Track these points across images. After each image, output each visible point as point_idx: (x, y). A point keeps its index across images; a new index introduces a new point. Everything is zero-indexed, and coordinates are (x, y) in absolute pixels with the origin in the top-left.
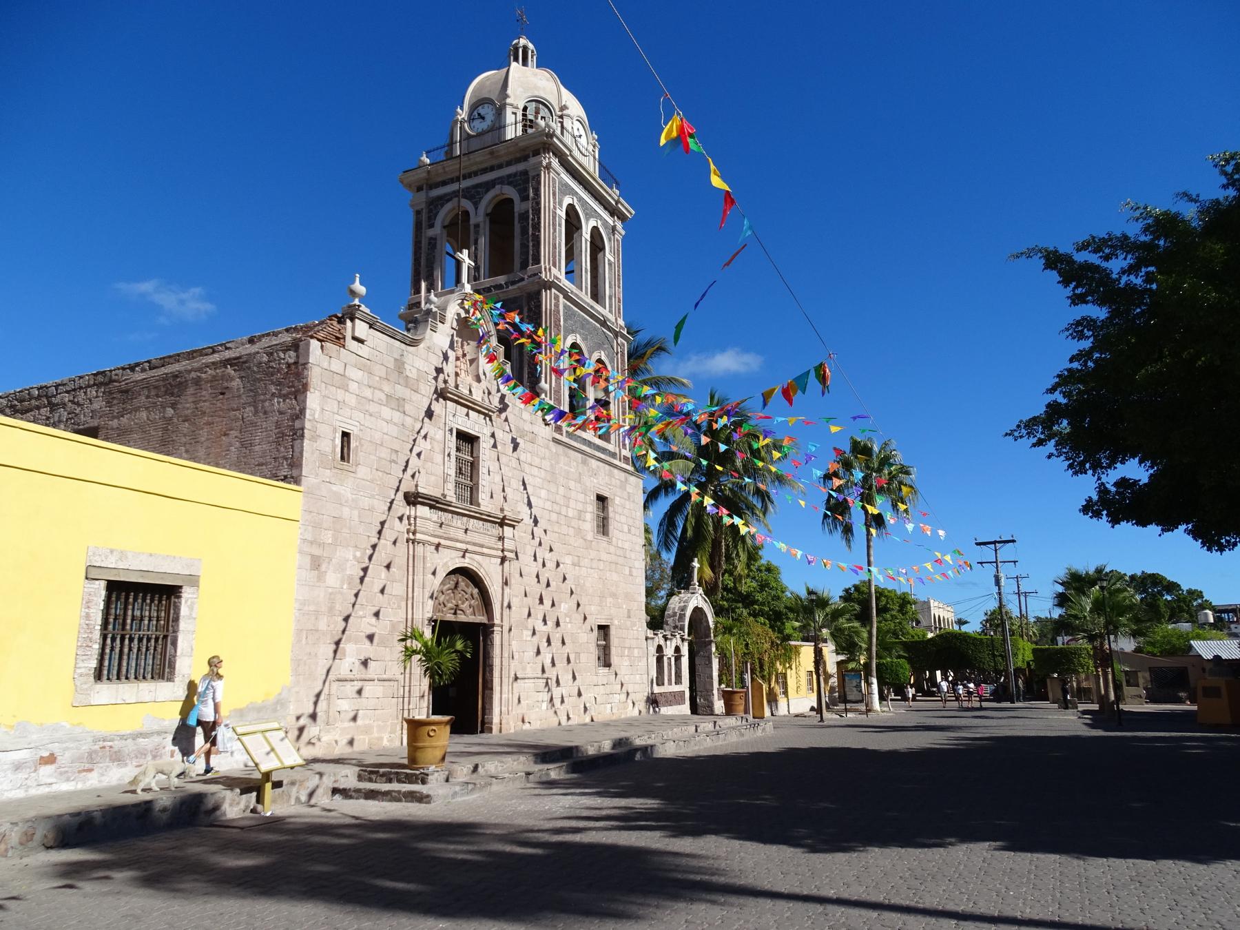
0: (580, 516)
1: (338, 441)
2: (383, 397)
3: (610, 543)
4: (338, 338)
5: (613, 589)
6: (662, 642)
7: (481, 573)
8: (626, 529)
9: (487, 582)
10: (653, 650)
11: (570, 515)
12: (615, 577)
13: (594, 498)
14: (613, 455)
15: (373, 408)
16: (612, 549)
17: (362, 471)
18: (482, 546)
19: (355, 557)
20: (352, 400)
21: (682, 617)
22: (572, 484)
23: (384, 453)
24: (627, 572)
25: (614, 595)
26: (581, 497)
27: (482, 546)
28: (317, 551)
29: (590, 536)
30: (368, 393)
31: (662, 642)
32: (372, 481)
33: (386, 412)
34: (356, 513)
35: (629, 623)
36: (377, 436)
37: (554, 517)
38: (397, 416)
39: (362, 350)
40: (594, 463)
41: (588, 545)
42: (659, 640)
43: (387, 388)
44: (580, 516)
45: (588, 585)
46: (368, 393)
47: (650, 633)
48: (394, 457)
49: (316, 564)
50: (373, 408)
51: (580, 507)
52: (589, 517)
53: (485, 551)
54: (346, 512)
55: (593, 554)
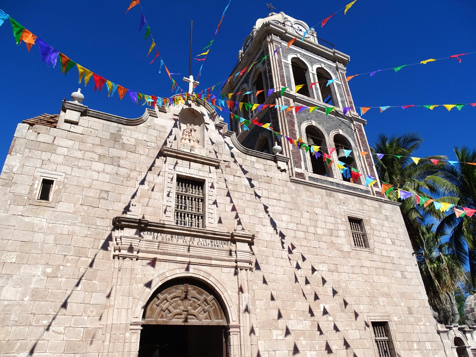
2: (96, 157)
3: (372, 253)
4: (52, 123)
5: (385, 290)
6: (459, 334)
7: (211, 281)
8: (389, 241)
9: (219, 289)
11: (320, 231)
12: (384, 280)
16: (375, 257)
18: (210, 259)
19: (44, 273)
20: (60, 159)
24: (399, 275)
25: (387, 295)
26: (332, 220)
27: (210, 259)
29: (347, 248)
30: (80, 155)
31: (459, 334)
32: (75, 213)
33: (99, 166)
34: (52, 237)
35: (412, 319)
36: (85, 182)
37: (301, 235)
38: (109, 168)
41: (346, 255)
42: (455, 332)
43: (100, 150)
44: (331, 233)
45: (351, 287)
47: (442, 327)
48: (105, 195)
50: (81, 163)
52: (342, 233)
53: (214, 262)
54: (38, 237)
55: (353, 262)
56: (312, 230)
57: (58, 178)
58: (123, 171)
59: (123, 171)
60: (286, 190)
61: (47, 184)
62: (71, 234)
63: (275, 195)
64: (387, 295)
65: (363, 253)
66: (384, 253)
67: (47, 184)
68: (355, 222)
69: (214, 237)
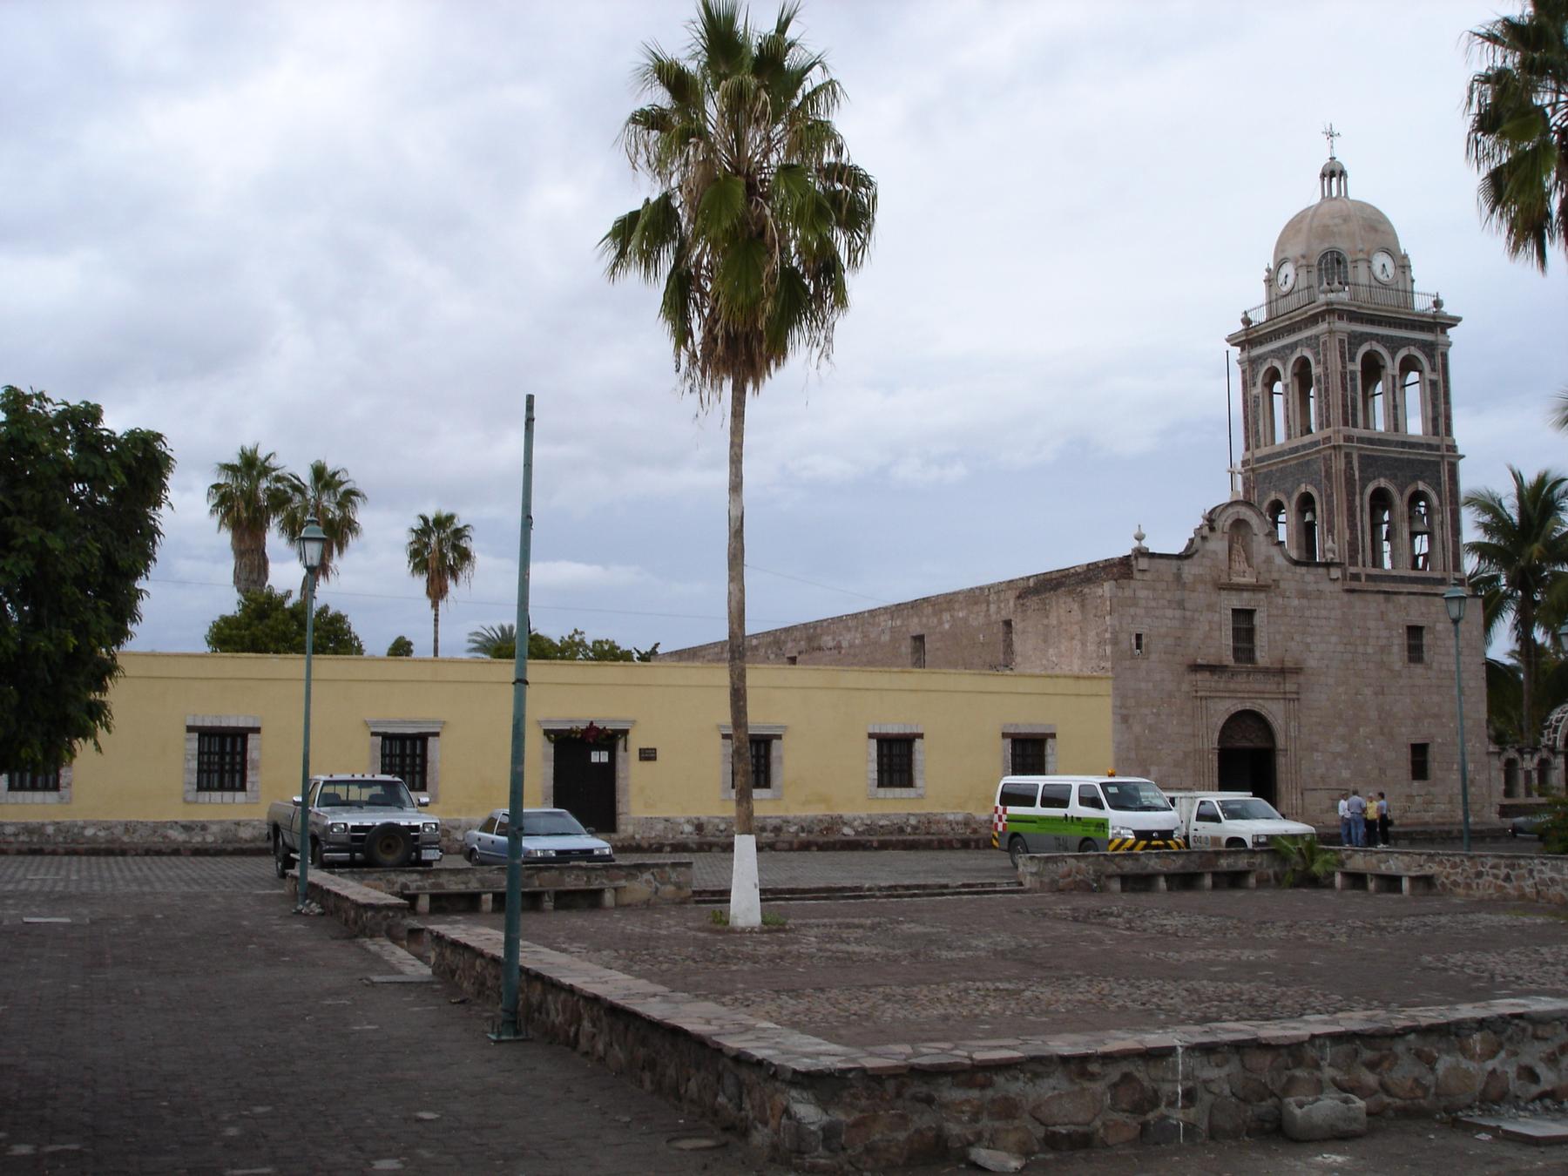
0: (1385, 649)
1: (1134, 641)
3: (1429, 667)
9: (1270, 718)
10: (1498, 764)
11: (1370, 650)
12: (1436, 698)
13: (1402, 631)
14: (1442, 582)
15: (1157, 613)
17: (1154, 657)
20: (1141, 611)
21: (1555, 731)
22: (1371, 624)
23: (1170, 641)
26: (1384, 633)
28: (1124, 712)
29: (1398, 666)
30: (1153, 604)
33: (1169, 613)
34: (1151, 685)
36: (1163, 630)
38: (1178, 613)
39: (1148, 576)
40: (1402, 599)
43: (1168, 596)
46: (1153, 604)
47: (1492, 748)
49: (1125, 719)
50: (1157, 613)
51: (1383, 642)
52: (1395, 649)
54: (1143, 685)
56: (1361, 649)
57: (1143, 630)
58: (1188, 614)
59: (1188, 614)
60: (1337, 603)
61: (1139, 637)
62: (1163, 680)
63: (1323, 613)
64: (1436, 716)
65: (1418, 669)
66: (1444, 667)
67: (1139, 637)
68: (1415, 632)
69: (1266, 671)
